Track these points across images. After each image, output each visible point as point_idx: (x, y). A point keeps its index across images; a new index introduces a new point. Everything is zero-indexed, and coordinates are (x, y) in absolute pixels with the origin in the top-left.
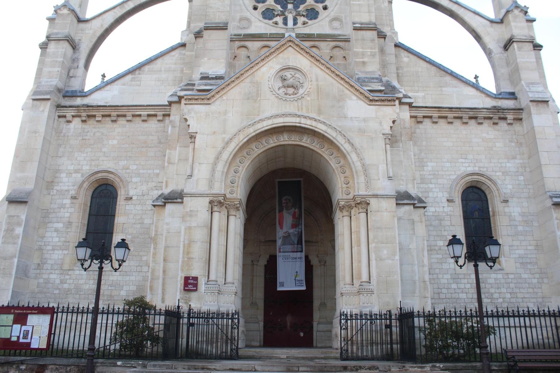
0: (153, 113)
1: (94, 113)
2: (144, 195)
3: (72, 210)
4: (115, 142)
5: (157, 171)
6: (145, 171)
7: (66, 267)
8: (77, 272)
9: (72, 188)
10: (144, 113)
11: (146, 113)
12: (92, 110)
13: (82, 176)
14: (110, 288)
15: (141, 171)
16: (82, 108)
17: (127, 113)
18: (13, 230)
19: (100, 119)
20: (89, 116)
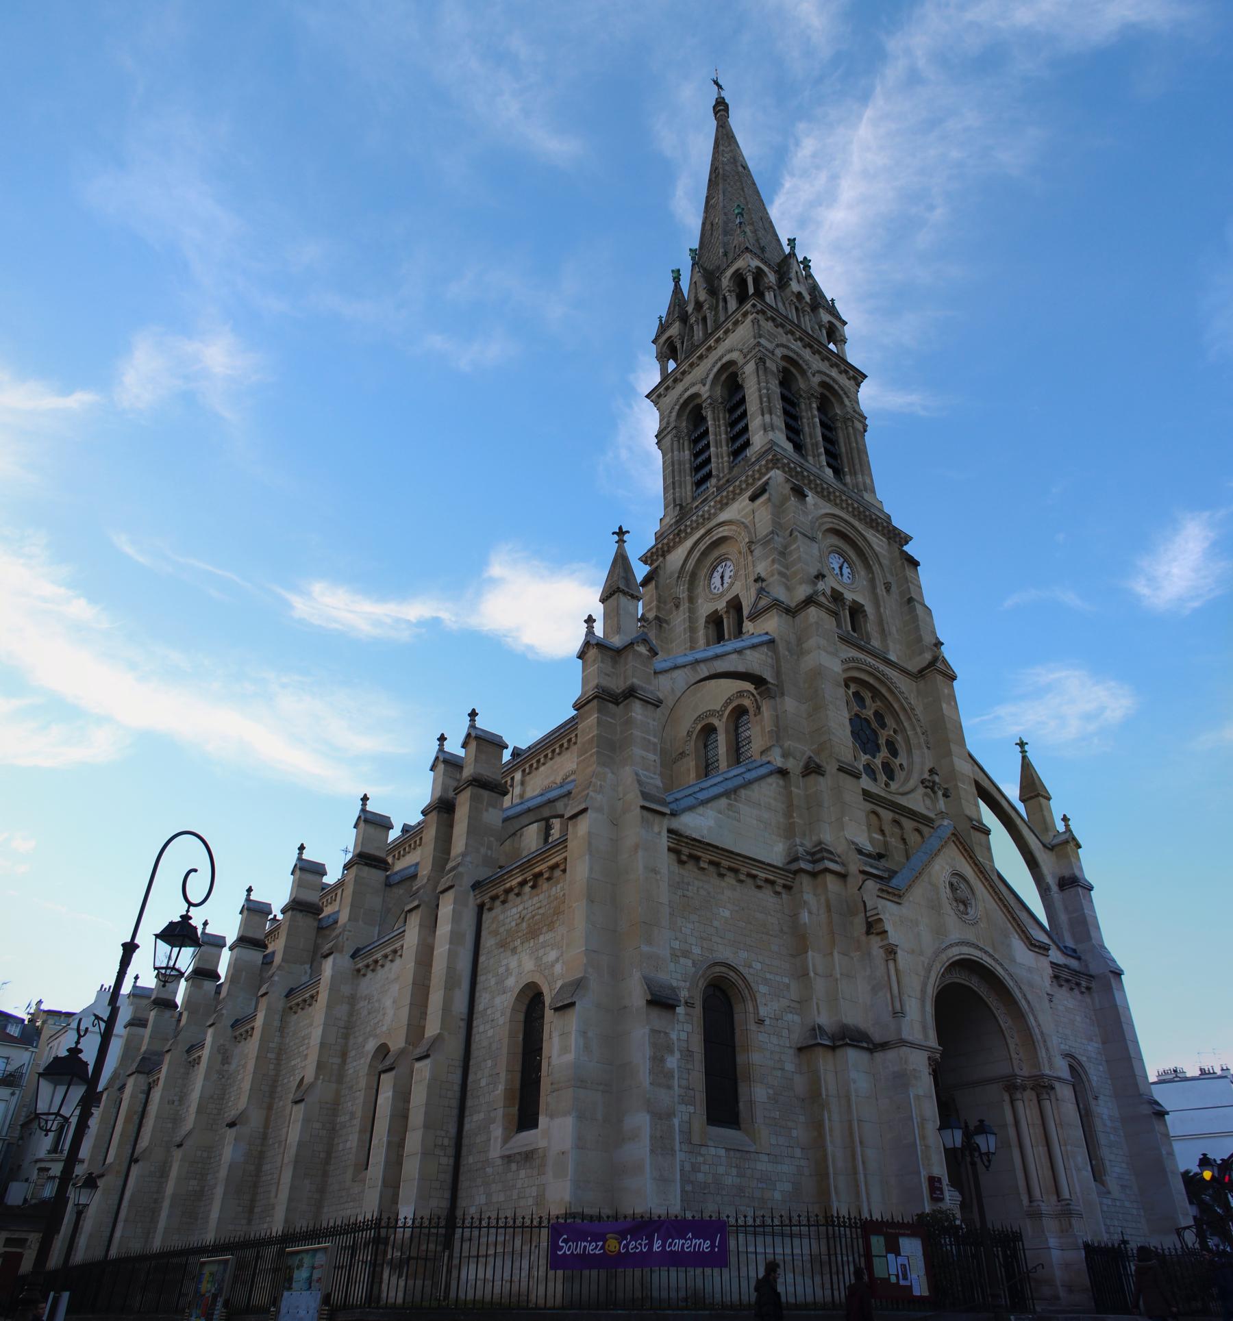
0: (772, 878)
1: (699, 854)
2: (777, 1020)
3: (688, 1027)
4: (727, 913)
5: (786, 980)
6: (771, 977)
7: (696, 1139)
8: (713, 1151)
9: (683, 984)
10: (725, 863)
11: (782, 881)
12: (699, 847)
13: (694, 964)
14: (760, 1185)
15: (768, 976)
16: (686, 840)
17: (742, 868)
18: (662, 1060)
19: (706, 866)
20: (691, 856)
